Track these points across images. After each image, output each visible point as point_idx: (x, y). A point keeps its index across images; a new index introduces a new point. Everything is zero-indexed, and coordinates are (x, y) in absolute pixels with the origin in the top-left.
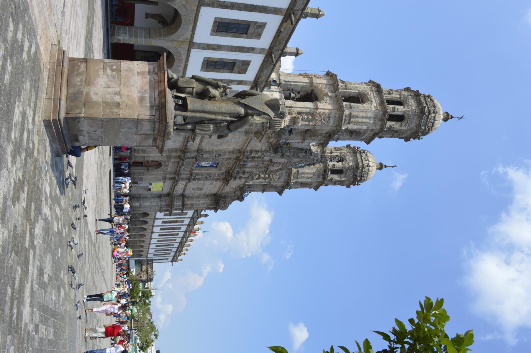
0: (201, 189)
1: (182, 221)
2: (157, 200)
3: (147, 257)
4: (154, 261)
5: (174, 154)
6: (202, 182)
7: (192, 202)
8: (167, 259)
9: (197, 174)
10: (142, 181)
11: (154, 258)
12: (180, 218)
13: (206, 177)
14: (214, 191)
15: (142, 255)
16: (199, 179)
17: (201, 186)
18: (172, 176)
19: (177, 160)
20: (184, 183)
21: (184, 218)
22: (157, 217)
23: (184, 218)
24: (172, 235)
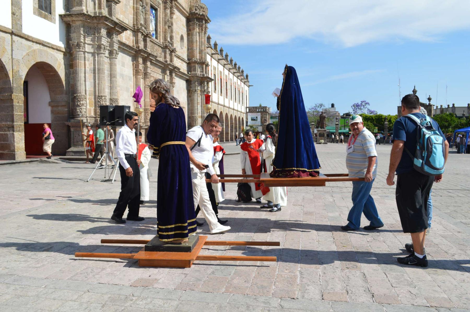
0: (182, 38)
4: (248, 106)
5: (141, 67)
9: (165, 39)
11: (245, 106)
12: (211, 70)
13: (169, 27)
14: (184, 20)
15: (243, 118)
16: (171, 38)
17: (179, 39)
18: (168, 72)
19: (149, 63)
20: (175, 59)
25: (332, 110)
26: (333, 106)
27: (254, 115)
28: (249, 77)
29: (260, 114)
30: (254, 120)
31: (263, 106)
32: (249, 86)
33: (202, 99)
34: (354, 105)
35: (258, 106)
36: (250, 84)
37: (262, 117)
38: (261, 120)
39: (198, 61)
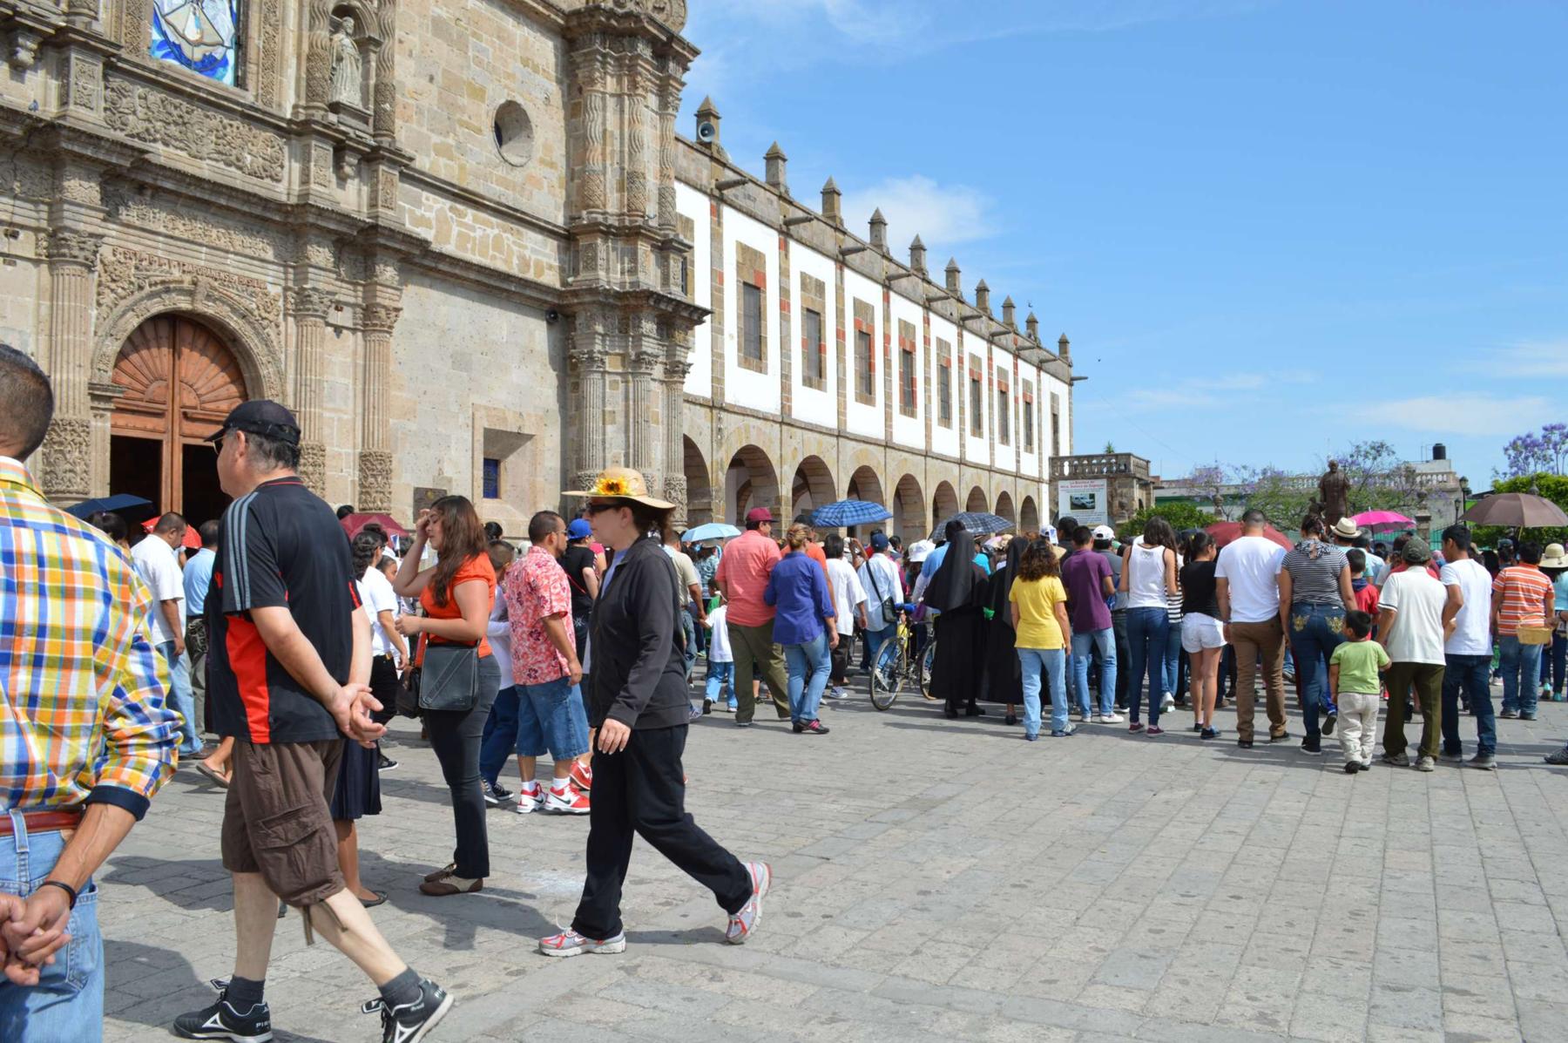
1: (813, 287)
2: (594, 386)
3: (1040, 481)
4: (1064, 451)
6: (404, 72)
7: (611, 179)
8: (1054, 398)
9: (312, 88)
10: (383, 459)
11: (1048, 452)
12: (784, 292)
15: (1028, 501)
21: (784, 273)
22: (772, 406)
23: (784, 273)
24: (907, 355)
25: (1439, 466)
26: (1439, 452)
27: (1082, 489)
28: (1070, 347)
29: (1104, 482)
30: (1083, 507)
31: (1117, 451)
32: (1071, 382)
33: (627, 399)
34: (1514, 445)
35: (1101, 451)
36: (1074, 373)
37: (1111, 496)
38: (1110, 504)
39: (613, 221)
